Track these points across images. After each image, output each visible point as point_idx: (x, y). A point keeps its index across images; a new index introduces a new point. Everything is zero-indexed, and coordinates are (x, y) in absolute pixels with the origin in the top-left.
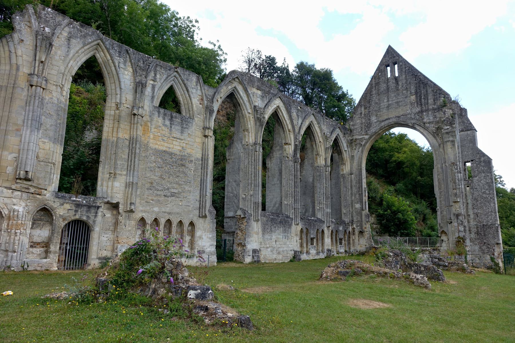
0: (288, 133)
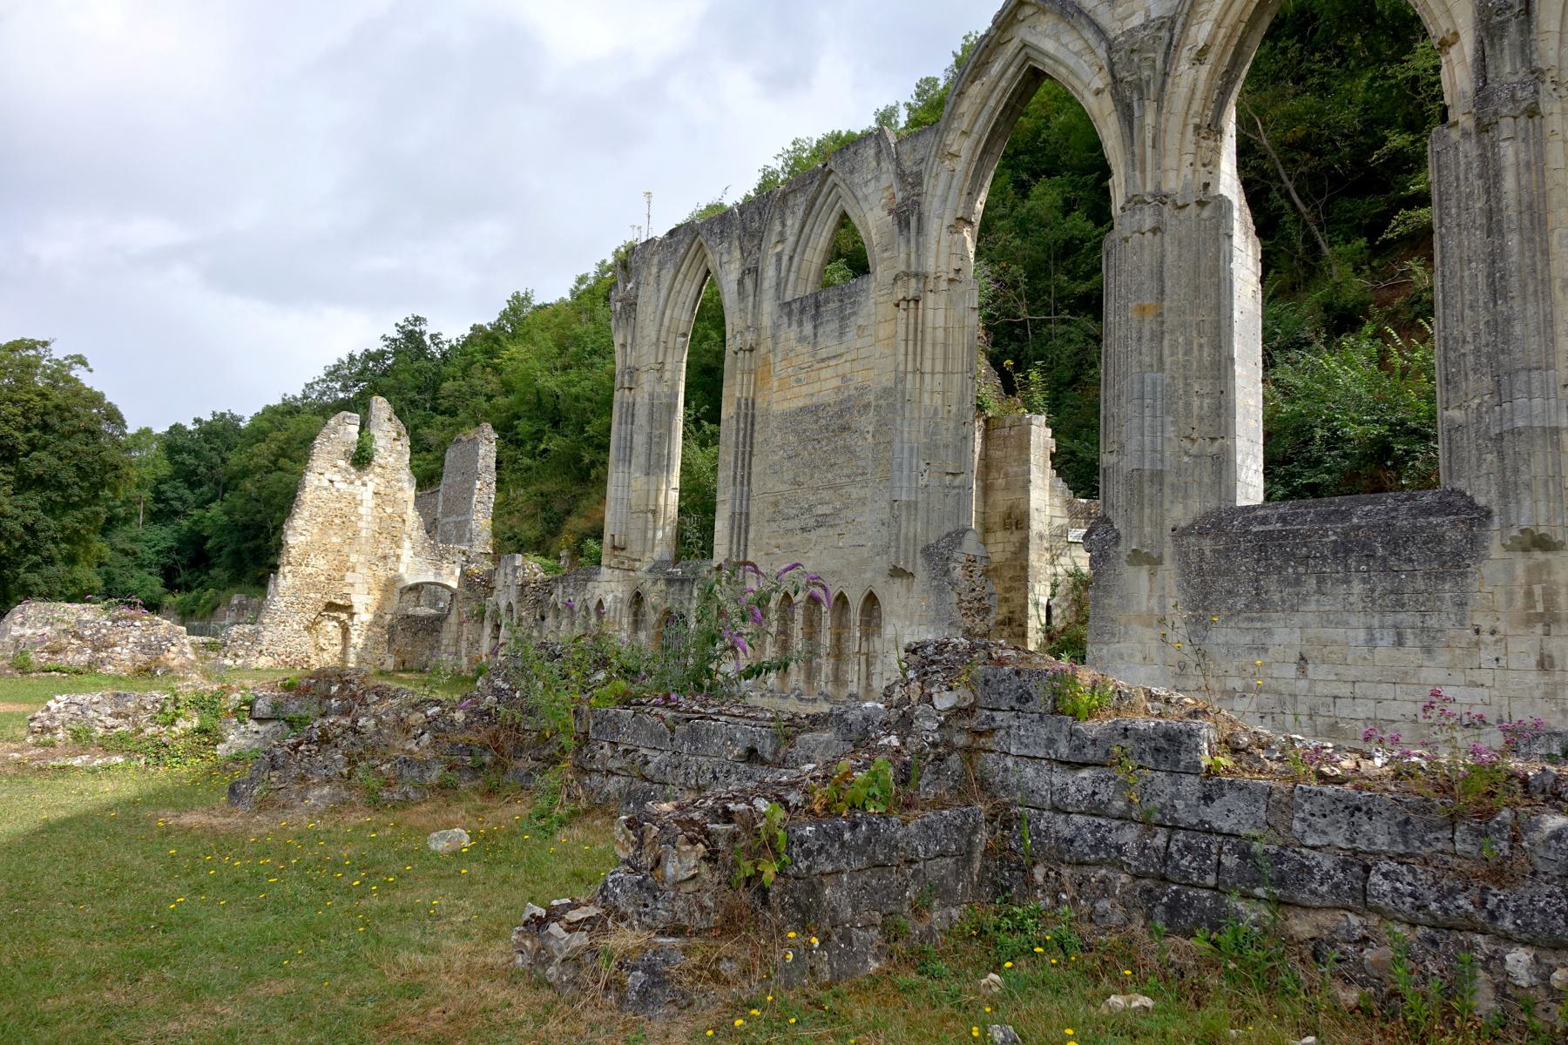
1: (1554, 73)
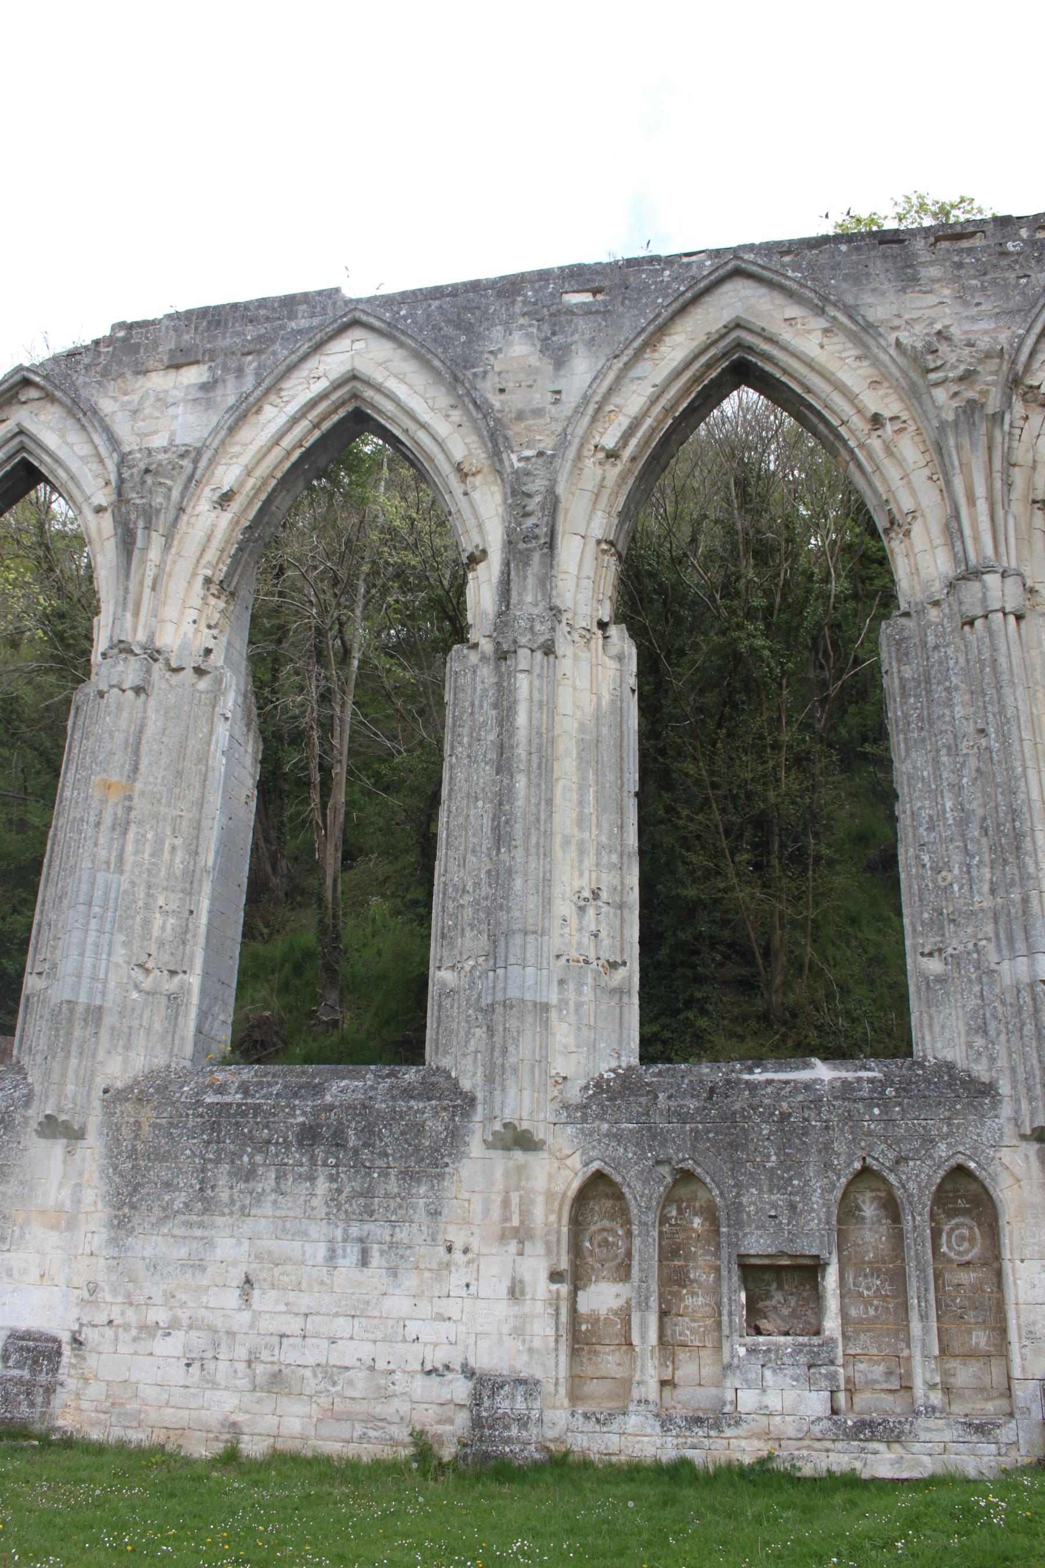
0: (457, 488)
1: (569, 615)
